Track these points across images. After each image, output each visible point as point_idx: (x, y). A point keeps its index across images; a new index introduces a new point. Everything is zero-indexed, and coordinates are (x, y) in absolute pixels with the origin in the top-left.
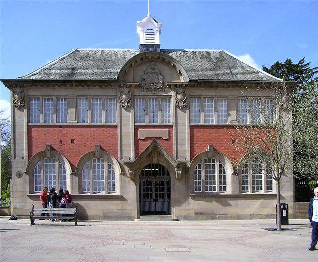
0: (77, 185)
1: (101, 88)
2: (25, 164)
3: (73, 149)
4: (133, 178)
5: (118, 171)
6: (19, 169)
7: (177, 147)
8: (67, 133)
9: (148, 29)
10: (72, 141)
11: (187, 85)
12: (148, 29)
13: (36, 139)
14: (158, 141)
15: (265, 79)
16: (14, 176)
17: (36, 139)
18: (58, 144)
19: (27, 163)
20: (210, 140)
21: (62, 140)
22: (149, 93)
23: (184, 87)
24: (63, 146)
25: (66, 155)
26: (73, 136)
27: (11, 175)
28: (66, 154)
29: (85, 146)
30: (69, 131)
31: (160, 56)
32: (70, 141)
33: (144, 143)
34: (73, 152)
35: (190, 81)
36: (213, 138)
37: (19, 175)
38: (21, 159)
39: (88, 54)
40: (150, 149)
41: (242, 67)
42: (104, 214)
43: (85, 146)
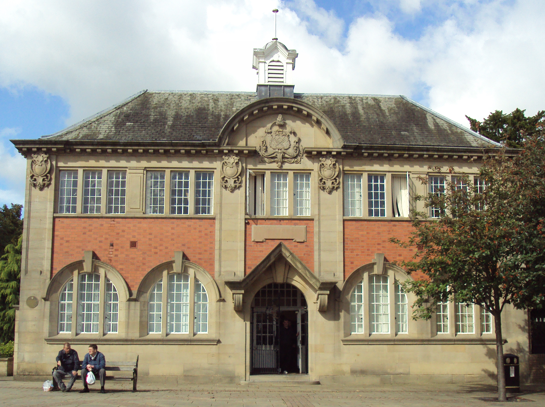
0: (138, 320)
1: (232, 94)
2: (45, 282)
3: (132, 258)
4: (239, 310)
5: (212, 295)
6: (32, 293)
7: (319, 255)
8: (123, 231)
9: (273, 61)
10: (133, 244)
11: (339, 153)
12: (273, 61)
13: (67, 241)
14: (286, 243)
15: (474, 144)
16: (23, 304)
17: (67, 241)
18: (106, 250)
19: (48, 282)
20: (379, 244)
21: (115, 242)
22: (274, 166)
23: (334, 156)
24: (116, 253)
25: (122, 269)
26: (134, 237)
27: (18, 303)
28: (120, 267)
29: (156, 253)
30: (129, 228)
31: (294, 105)
32: (129, 245)
33: (259, 247)
34: (133, 264)
35: (344, 147)
36: (384, 241)
37: (33, 303)
38: (37, 275)
39: (167, 99)
40: (273, 259)
41: (436, 125)
42: (184, 371)
43: (156, 253)
